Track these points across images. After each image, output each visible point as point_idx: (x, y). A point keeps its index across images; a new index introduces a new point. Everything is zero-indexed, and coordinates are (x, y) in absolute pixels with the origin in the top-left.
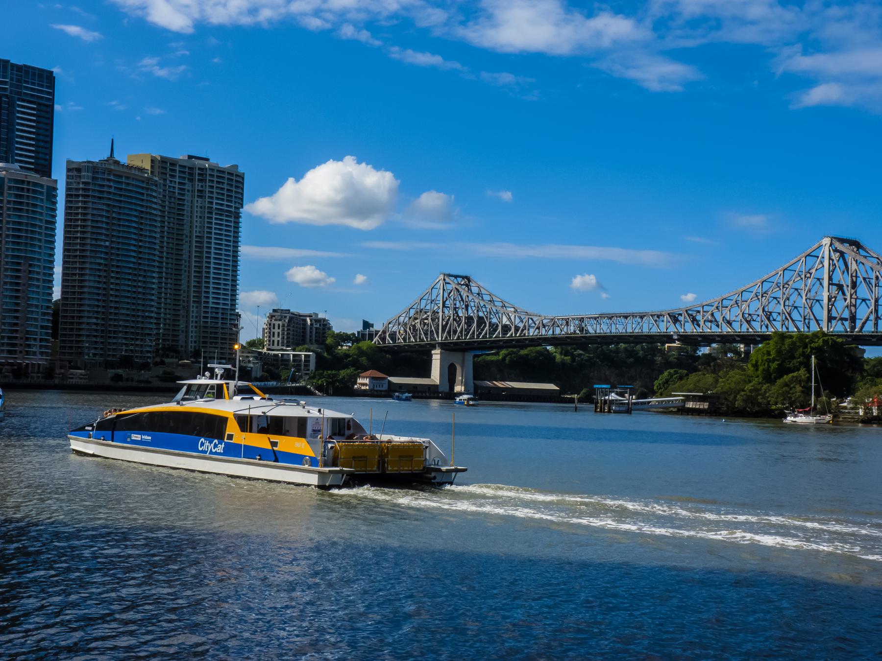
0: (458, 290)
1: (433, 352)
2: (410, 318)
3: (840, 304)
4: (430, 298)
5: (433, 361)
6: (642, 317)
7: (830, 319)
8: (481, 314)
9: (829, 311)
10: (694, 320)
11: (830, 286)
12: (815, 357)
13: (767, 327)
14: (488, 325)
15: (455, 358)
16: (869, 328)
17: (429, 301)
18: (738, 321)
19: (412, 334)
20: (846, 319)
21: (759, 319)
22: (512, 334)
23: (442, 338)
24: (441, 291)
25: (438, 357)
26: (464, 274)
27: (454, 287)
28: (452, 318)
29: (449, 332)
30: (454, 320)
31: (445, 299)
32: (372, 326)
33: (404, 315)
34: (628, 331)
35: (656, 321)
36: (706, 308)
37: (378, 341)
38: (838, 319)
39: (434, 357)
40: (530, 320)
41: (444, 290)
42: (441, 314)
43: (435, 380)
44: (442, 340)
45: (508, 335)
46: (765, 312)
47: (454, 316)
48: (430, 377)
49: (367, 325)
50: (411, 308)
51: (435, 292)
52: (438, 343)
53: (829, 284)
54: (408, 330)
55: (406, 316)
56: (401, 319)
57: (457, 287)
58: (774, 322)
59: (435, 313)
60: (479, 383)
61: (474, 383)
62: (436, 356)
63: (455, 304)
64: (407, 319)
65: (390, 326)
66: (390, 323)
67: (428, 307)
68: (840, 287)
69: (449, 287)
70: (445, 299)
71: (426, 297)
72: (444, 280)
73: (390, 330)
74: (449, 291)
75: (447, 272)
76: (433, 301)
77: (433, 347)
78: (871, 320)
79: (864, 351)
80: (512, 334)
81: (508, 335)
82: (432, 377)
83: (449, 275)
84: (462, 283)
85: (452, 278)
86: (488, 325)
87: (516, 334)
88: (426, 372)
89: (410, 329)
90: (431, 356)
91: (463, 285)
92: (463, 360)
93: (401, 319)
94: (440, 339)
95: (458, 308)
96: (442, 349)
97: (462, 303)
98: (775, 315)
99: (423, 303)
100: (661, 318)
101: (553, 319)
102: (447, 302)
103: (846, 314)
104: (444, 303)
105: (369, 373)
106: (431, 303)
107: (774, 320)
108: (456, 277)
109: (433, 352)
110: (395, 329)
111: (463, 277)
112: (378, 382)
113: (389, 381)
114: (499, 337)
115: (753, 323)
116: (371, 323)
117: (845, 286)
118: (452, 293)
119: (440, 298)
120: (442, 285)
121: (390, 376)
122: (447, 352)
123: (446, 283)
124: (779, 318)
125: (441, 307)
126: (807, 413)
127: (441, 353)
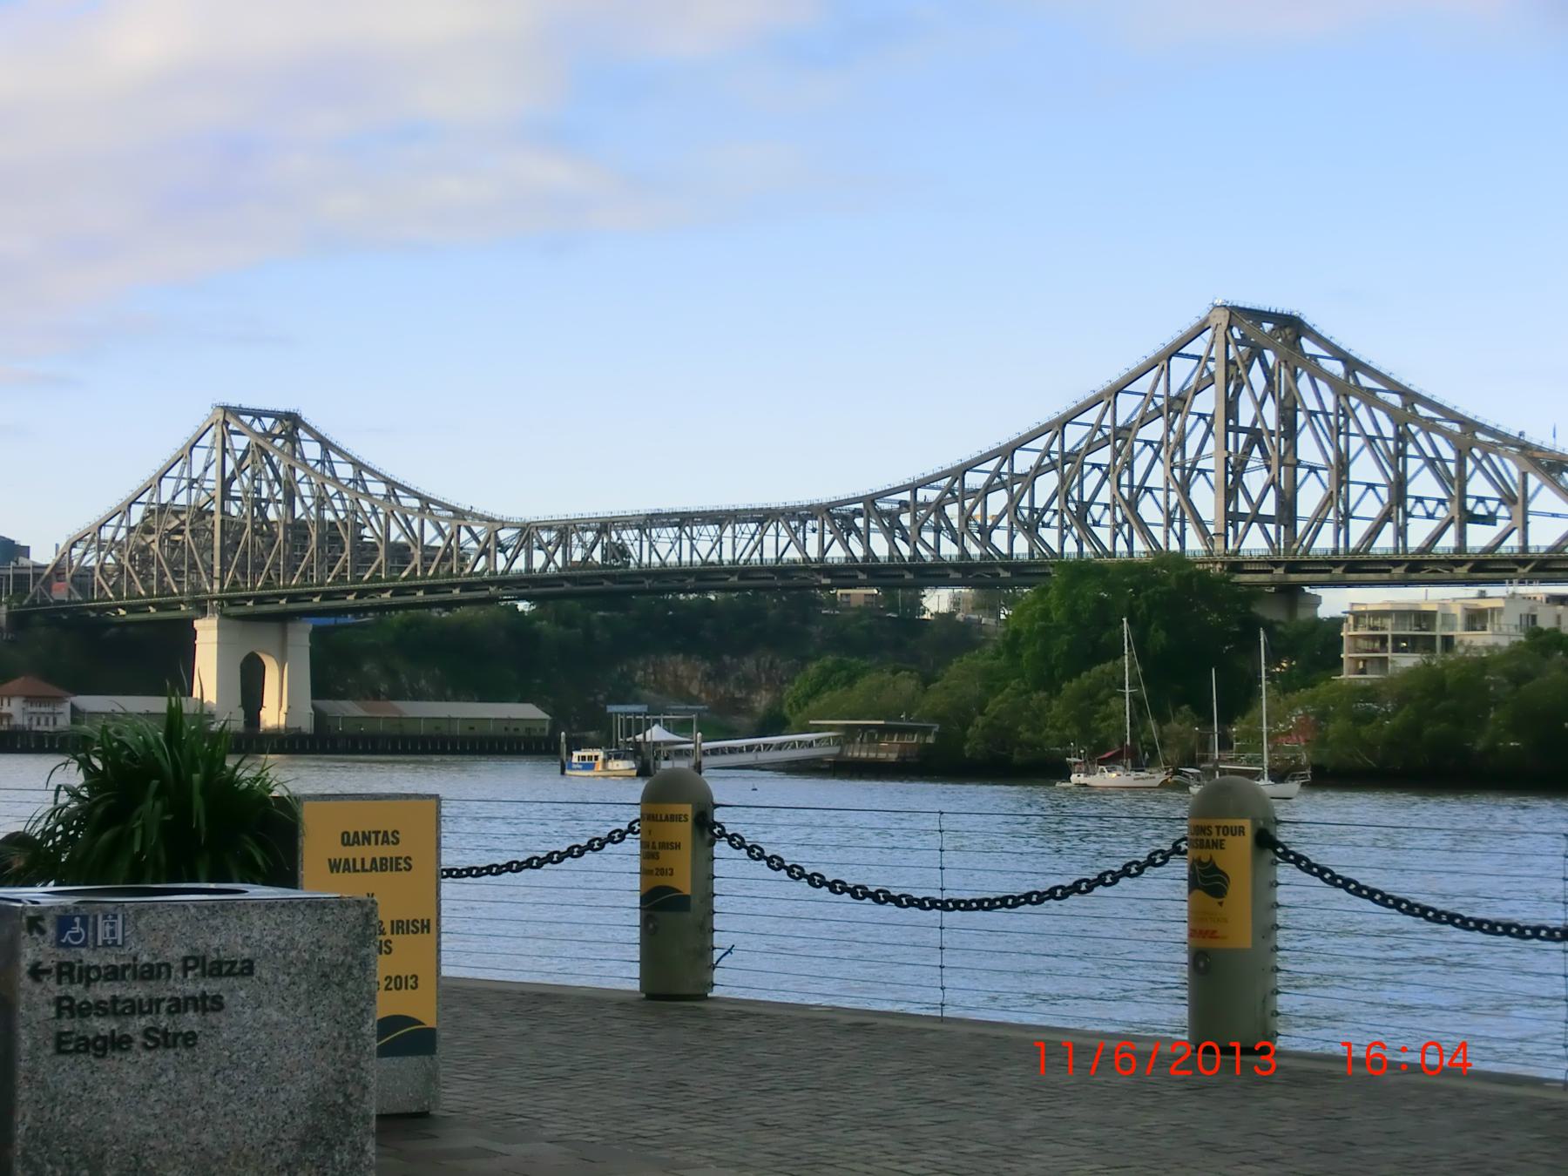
0: (265, 453)
2: (130, 530)
3: (1255, 480)
4: (185, 475)
6: (761, 522)
7: (1232, 518)
8: (329, 516)
9: (1230, 494)
10: (892, 526)
11: (1231, 435)
12: (1128, 621)
13: (1079, 542)
14: (348, 547)
15: (261, 642)
16: (1325, 541)
17: (184, 483)
18: (1003, 528)
19: (138, 573)
20: (1269, 519)
21: (1055, 522)
22: (415, 569)
23: (222, 585)
24: (216, 454)
26: (282, 406)
27: (253, 442)
28: (248, 529)
29: (242, 568)
30: (255, 532)
31: (228, 474)
32: (25, 551)
33: (115, 521)
34: (724, 558)
35: (793, 533)
36: (922, 494)
37: (42, 593)
38: (1250, 518)
40: (463, 529)
41: (224, 451)
42: (217, 518)
44: (221, 591)
45: (405, 574)
46: (1074, 501)
47: (253, 523)
50: (134, 502)
51: (199, 456)
53: (1228, 429)
54: (126, 563)
55: (119, 526)
56: (107, 533)
57: (261, 442)
58: (1094, 528)
59: (201, 513)
60: (329, 706)
61: (313, 707)
62: (207, 633)
63: (259, 491)
64: (122, 533)
65: (75, 552)
66: (74, 545)
67: (181, 500)
68: (1255, 436)
69: (240, 443)
70: (228, 474)
71: (175, 472)
72: (226, 423)
73: (75, 563)
74: (239, 454)
75: (234, 403)
76: (196, 481)
77: (203, 612)
79: (1317, 601)
80: (415, 569)
81: (405, 574)
83: (238, 412)
84: (276, 431)
85: (247, 419)
86: (348, 547)
87: (426, 569)
89: (132, 558)
91: (279, 436)
93: (107, 533)
94: (217, 586)
95: (264, 500)
96: (224, 616)
97: (277, 488)
98: (1096, 511)
99: (168, 487)
100: (810, 524)
101: (523, 529)
102: (236, 485)
103: (1269, 507)
104: (226, 484)
105: (14, 685)
106: (190, 487)
107: (1097, 524)
108: (258, 414)
109: (197, 624)
110: (91, 561)
111: (279, 416)
112: (43, 709)
113: (74, 709)
114: (379, 579)
115: (1043, 532)
116: (22, 544)
117: (1264, 432)
118: (248, 461)
119: (213, 473)
120: (219, 437)
121: (76, 694)
122: (238, 623)
124: (1106, 520)
125: (218, 499)
126: (1111, 762)
127: (219, 627)
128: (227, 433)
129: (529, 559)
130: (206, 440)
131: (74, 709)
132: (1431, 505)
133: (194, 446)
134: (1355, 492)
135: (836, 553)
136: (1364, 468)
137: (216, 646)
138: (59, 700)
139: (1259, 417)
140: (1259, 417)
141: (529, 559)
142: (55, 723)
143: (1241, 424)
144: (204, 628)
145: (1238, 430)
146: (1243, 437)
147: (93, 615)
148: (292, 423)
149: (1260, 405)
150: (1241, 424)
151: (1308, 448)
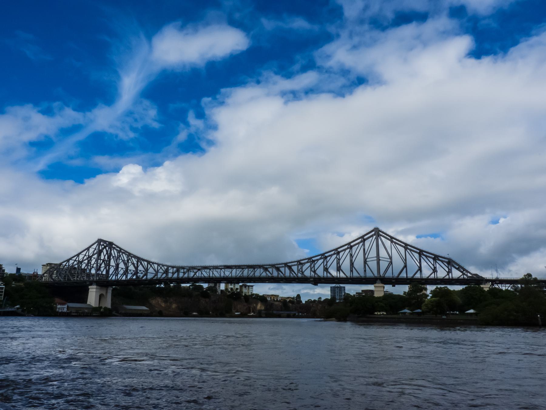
1: (90, 287)
4: (87, 254)
5: (89, 293)
25: (95, 290)
39: (90, 290)
43: (92, 305)
48: (86, 303)
49: (18, 270)
51: (91, 250)
52: (94, 281)
75: (102, 239)
77: (91, 284)
78: (449, 272)
82: (88, 303)
88: (84, 299)
90: (88, 289)
92: (107, 293)
96: (97, 285)
109: (90, 287)
123: (102, 245)
127: (96, 288)
128: (99, 245)
129: (178, 275)
130: (94, 246)
131: (68, 307)
132: (142, 272)
133: (90, 247)
134: (120, 269)
135: (264, 274)
136: (122, 265)
137: (95, 292)
138: (64, 304)
139: (105, 258)
140: (105, 258)
141: (178, 275)
142: (63, 310)
143: (101, 259)
144: (91, 288)
145: (100, 260)
146: (101, 261)
147: (56, 285)
148: (110, 245)
149: (105, 256)
150: (101, 259)
151: (112, 263)
